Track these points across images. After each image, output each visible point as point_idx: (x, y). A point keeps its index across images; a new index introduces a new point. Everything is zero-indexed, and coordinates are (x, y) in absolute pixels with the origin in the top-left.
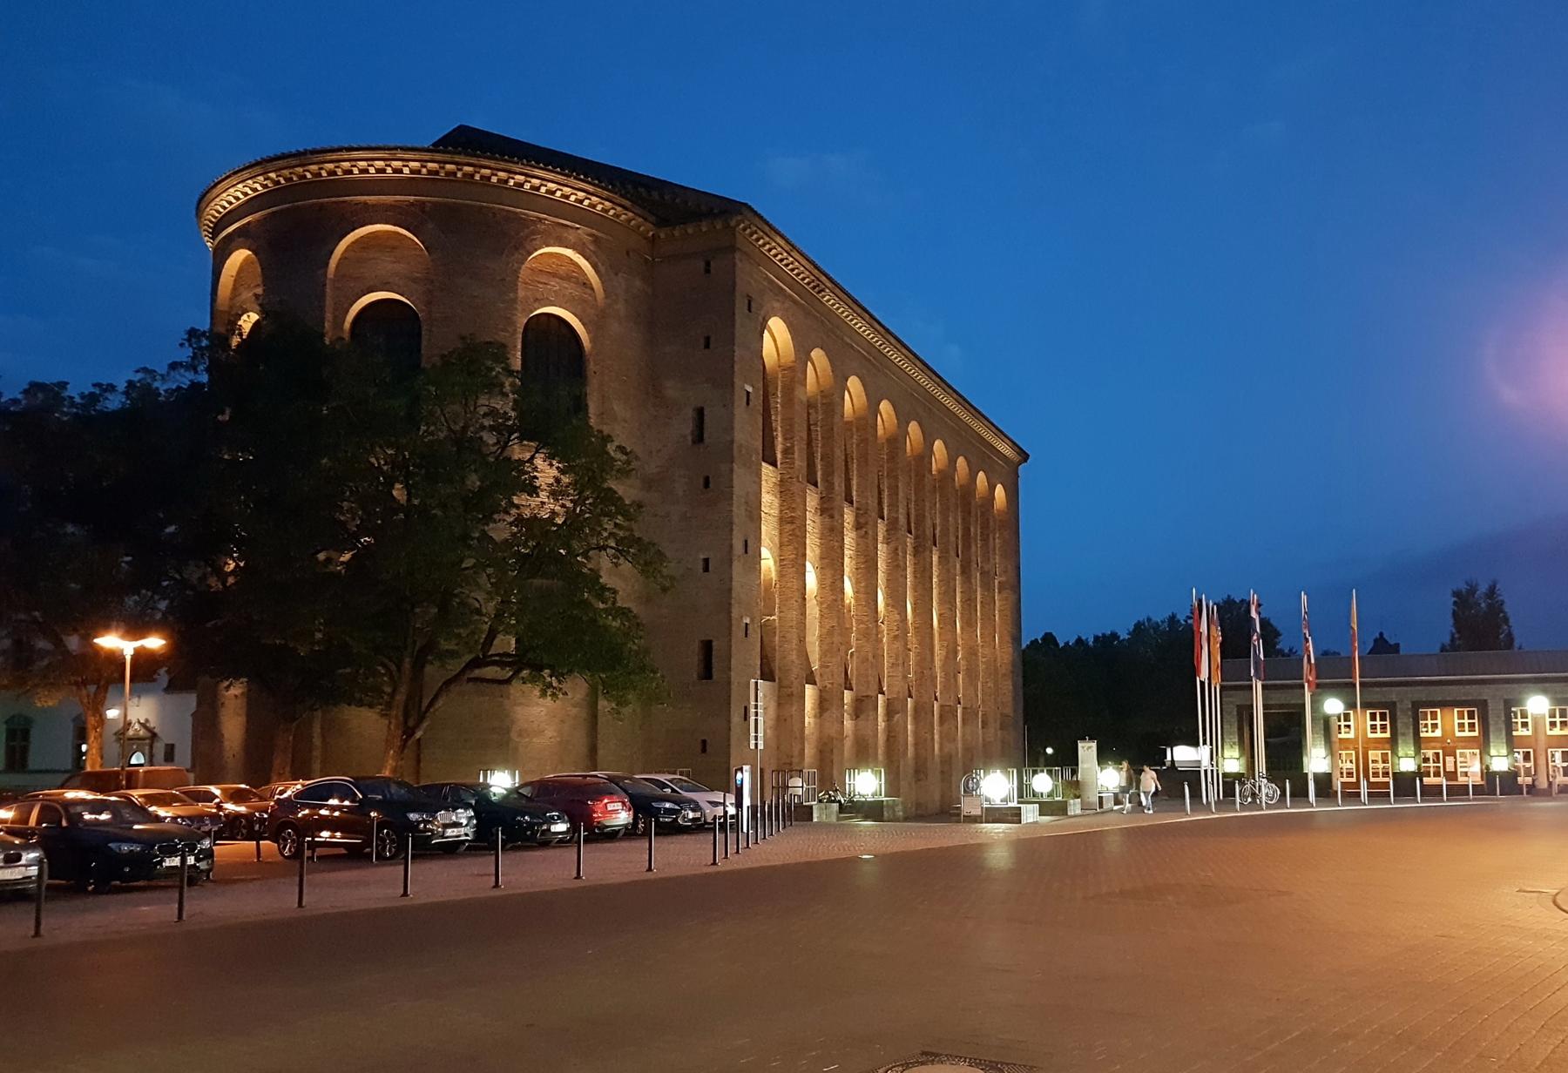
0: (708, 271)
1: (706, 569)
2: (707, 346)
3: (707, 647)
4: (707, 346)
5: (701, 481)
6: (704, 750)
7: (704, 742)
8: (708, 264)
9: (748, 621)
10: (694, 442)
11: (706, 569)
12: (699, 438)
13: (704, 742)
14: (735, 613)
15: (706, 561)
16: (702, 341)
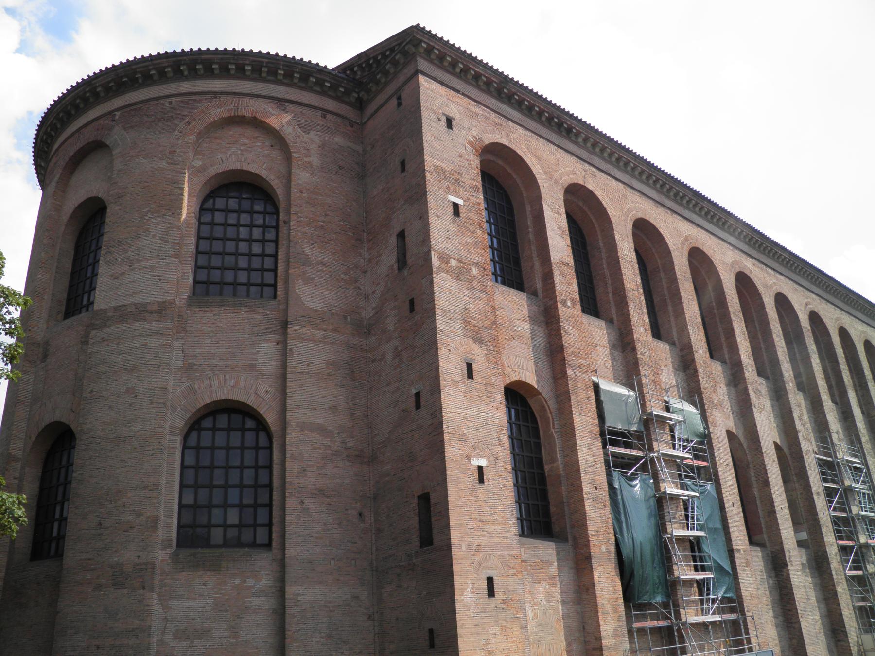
0: (399, 104)
1: (418, 406)
2: (403, 169)
3: (425, 499)
4: (403, 169)
5: (407, 306)
6: (432, 645)
7: (431, 631)
8: (399, 98)
9: (483, 462)
10: (399, 269)
11: (418, 406)
12: (402, 262)
13: (431, 631)
14: (453, 451)
15: (418, 395)
16: (399, 168)
